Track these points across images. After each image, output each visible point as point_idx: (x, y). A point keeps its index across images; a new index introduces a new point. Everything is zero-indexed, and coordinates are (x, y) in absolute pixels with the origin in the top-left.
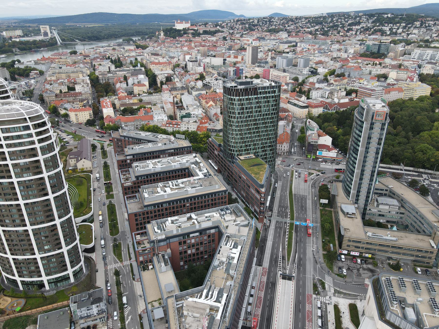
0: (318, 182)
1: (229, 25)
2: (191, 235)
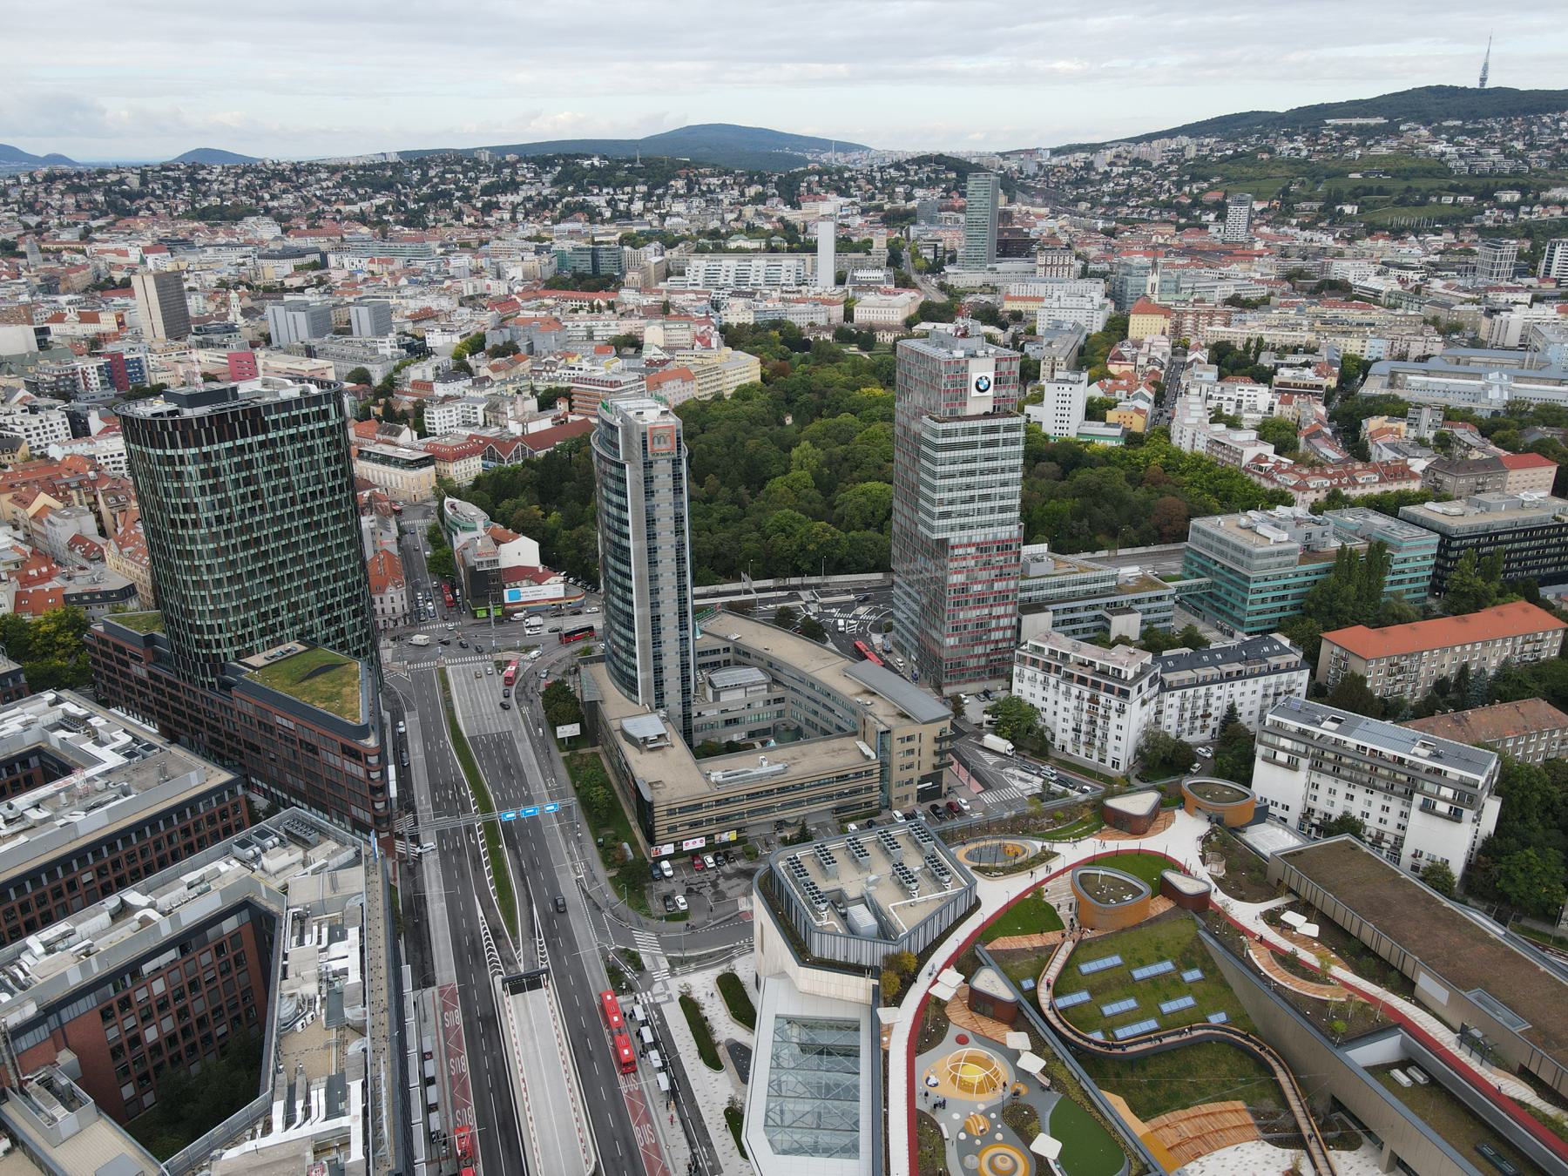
0: (532, 684)
2: (147, 968)
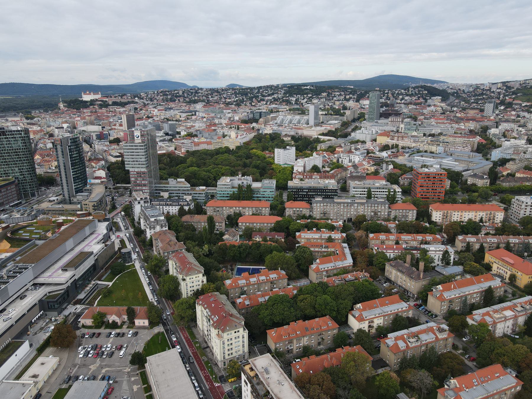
1: (149, 96)
